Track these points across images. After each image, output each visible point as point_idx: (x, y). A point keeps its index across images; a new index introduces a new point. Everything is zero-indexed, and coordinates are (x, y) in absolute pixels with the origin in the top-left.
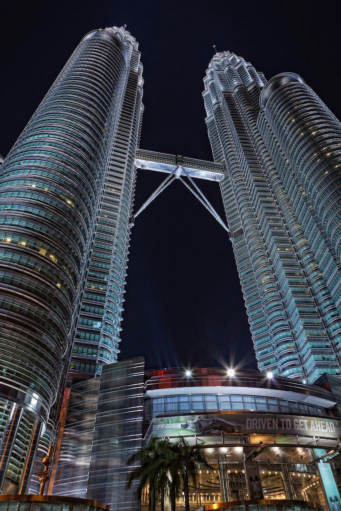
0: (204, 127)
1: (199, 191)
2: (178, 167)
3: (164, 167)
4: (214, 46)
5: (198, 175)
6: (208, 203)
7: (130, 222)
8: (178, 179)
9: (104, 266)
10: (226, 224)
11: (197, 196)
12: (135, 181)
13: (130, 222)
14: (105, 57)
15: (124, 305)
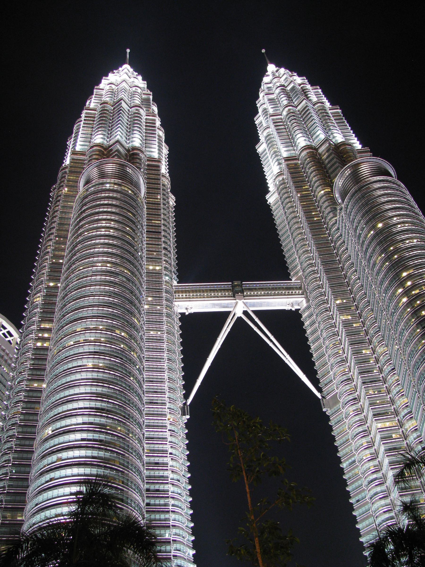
0: (267, 208)
1: (272, 338)
2: (237, 303)
3: (217, 305)
4: (263, 51)
5: (268, 305)
6: (288, 356)
7: (184, 414)
8: (241, 317)
9: (163, 516)
10: (316, 382)
11: (271, 344)
12: (175, 256)
13: (184, 414)
14: (114, 171)
15: (195, 545)
